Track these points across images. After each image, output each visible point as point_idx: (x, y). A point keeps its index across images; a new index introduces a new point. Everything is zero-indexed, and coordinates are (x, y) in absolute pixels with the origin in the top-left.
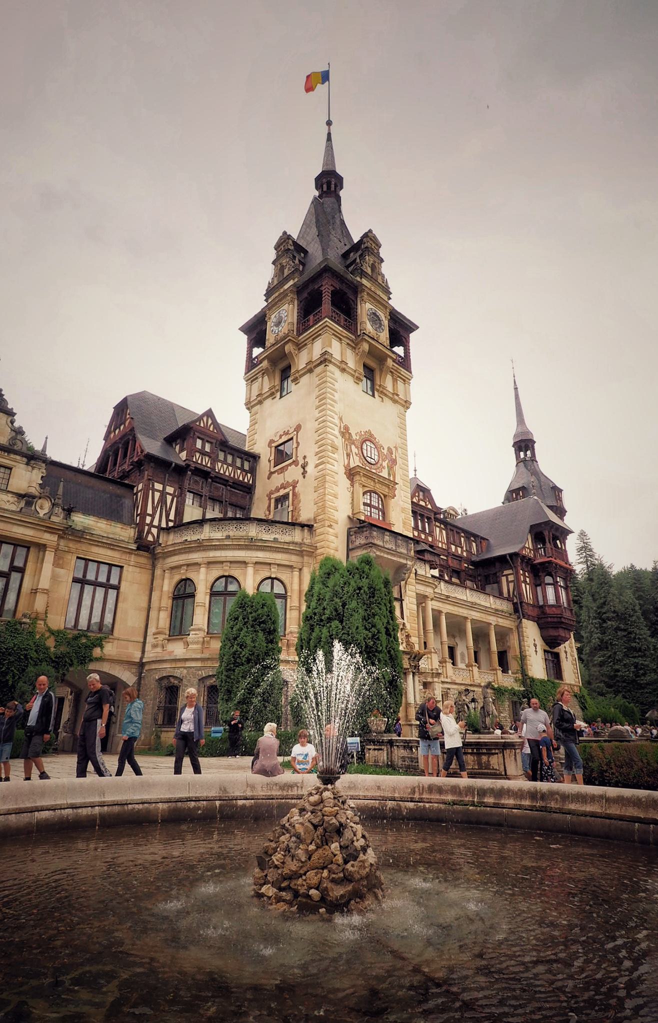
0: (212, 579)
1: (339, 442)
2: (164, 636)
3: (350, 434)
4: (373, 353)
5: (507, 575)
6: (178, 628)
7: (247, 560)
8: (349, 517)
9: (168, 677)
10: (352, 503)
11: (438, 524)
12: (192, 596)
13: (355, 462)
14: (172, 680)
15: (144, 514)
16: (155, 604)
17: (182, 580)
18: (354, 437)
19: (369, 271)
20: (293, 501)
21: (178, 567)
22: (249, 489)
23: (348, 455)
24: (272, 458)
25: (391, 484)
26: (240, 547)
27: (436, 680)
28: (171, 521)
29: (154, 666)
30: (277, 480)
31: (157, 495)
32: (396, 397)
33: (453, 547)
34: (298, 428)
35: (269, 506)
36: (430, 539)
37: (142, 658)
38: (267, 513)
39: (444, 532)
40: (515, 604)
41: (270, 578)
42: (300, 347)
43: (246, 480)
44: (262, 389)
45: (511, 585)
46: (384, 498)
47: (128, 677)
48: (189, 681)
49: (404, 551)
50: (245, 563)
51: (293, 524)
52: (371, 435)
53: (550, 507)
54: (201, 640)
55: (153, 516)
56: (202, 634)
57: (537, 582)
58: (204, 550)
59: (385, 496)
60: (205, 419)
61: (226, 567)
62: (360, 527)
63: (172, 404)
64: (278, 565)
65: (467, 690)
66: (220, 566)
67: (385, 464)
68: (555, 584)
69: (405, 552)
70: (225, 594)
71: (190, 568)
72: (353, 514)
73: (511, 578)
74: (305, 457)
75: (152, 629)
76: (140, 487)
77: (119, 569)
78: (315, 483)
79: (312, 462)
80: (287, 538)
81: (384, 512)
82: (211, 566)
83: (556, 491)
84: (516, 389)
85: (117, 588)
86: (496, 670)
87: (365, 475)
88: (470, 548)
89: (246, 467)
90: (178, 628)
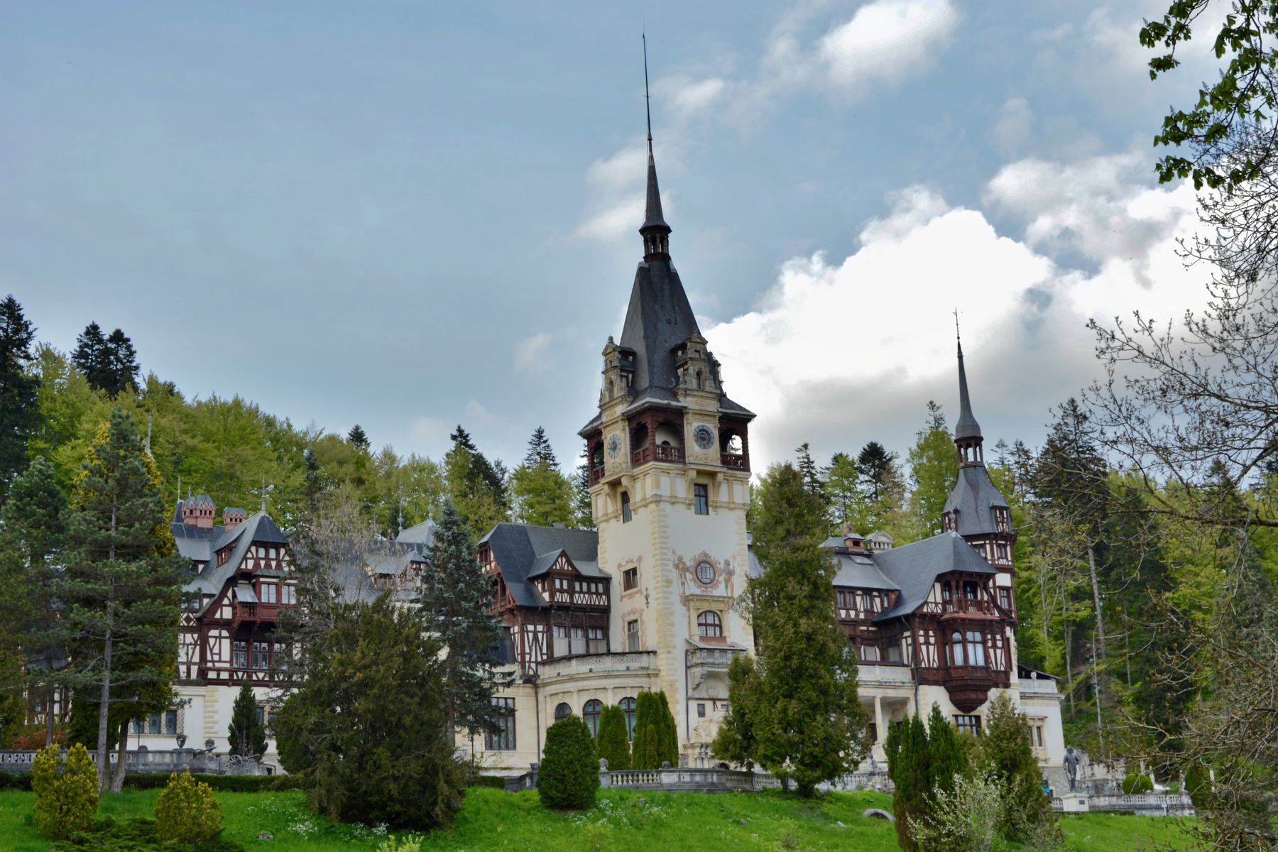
1: (674, 575)
4: (699, 473)
15: (523, 654)
19: (693, 383)
22: (605, 611)
23: (683, 584)
26: (601, 677)
31: (531, 635)
42: (634, 478)
52: (706, 555)
55: (530, 654)
57: (944, 643)
67: (722, 578)
73: (909, 641)
84: (960, 357)
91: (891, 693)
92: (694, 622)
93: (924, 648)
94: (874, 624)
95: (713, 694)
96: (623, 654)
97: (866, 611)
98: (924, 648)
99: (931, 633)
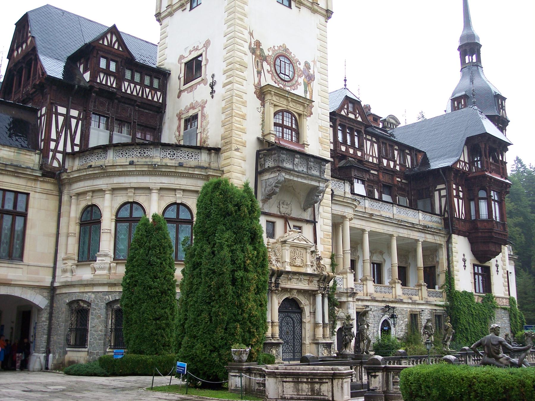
0: (117, 206)
1: (249, 59)
2: (73, 262)
3: (262, 50)
5: (439, 190)
6: (87, 253)
7: (151, 186)
8: (258, 139)
9: (77, 301)
10: (263, 125)
11: (369, 137)
12: (99, 222)
13: (267, 79)
14: (82, 304)
16: (63, 230)
17: (88, 206)
18: (266, 53)
20: (202, 122)
21: (84, 193)
22: (159, 109)
23: (259, 73)
24: (182, 75)
25: (307, 103)
26: (143, 173)
27: (350, 299)
28: (77, 145)
29: (64, 291)
30: (187, 99)
31: (61, 119)
32: (316, 7)
33: (385, 162)
34: (207, 44)
35: (179, 126)
36: (359, 154)
37: (53, 282)
38: (177, 133)
39: (376, 146)
40: (445, 220)
41: (175, 203)
43: (155, 99)
44: (160, 8)
45: (443, 200)
46: (297, 118)
47: (40, 300)
48: (97, 305)
49: (316, 173)
50: (149, 189)
51: (200, 148)
52: (286, 50)
53: (491, 118)
54: (108, 266)
55: (57, 141)
56: (108, 260)
57: (471, 198)
58: (108, 176)
59: (300, 115)
60: (109, 36)
61: (131, 193)
62: (268, 151)
63: (79, 17)
64: (184, 190)
65: (387, 307)
66: (124, 192)
67: (301, 80)
68: (488, 199)
69: (317, 174)
70: (131, 220)
71: (95, 194)
72: (264, 136)
73: (443, 193)
74: (213, 76)
75: (61, 255)
76: (44, 110)
77: (25, 196)
78: (223, 104)
79: (220, 79)
80: (193, 162)
81: (297, 131)
82: (116, 192)
83: (499, 100)
85: (25, 215)
86: (420, 285)
87: (276, 94)
88: (405, 162)
89: (156, 84)
90: (87, 253)
91: (430, 238)
92: (271, 120)
93: (456, 200)
94: (406, 177)
95: (284, 210)
96: (177, 147)
97: (400, 164)
98: (456, 200)
99: (460, 189)
